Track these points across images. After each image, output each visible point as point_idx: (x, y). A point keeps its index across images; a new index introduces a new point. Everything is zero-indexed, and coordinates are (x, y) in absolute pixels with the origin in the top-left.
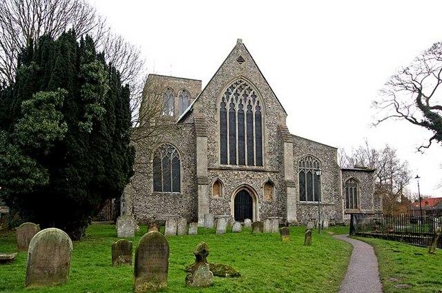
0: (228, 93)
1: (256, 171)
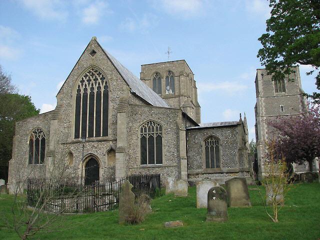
0: (82, 81)
1: (100, 141)
